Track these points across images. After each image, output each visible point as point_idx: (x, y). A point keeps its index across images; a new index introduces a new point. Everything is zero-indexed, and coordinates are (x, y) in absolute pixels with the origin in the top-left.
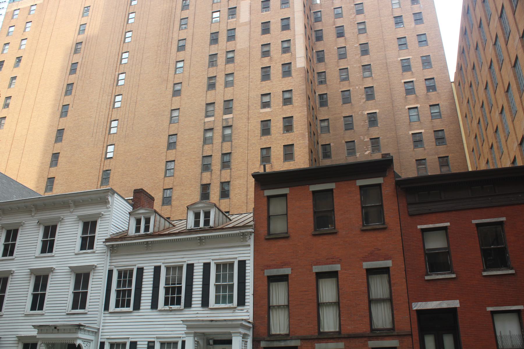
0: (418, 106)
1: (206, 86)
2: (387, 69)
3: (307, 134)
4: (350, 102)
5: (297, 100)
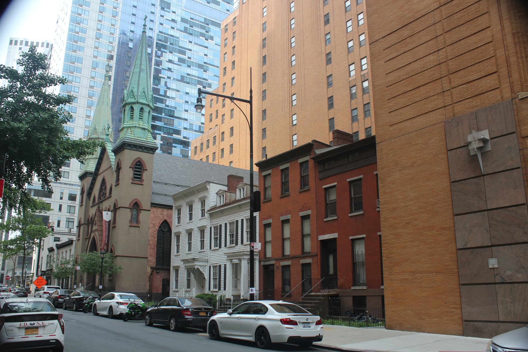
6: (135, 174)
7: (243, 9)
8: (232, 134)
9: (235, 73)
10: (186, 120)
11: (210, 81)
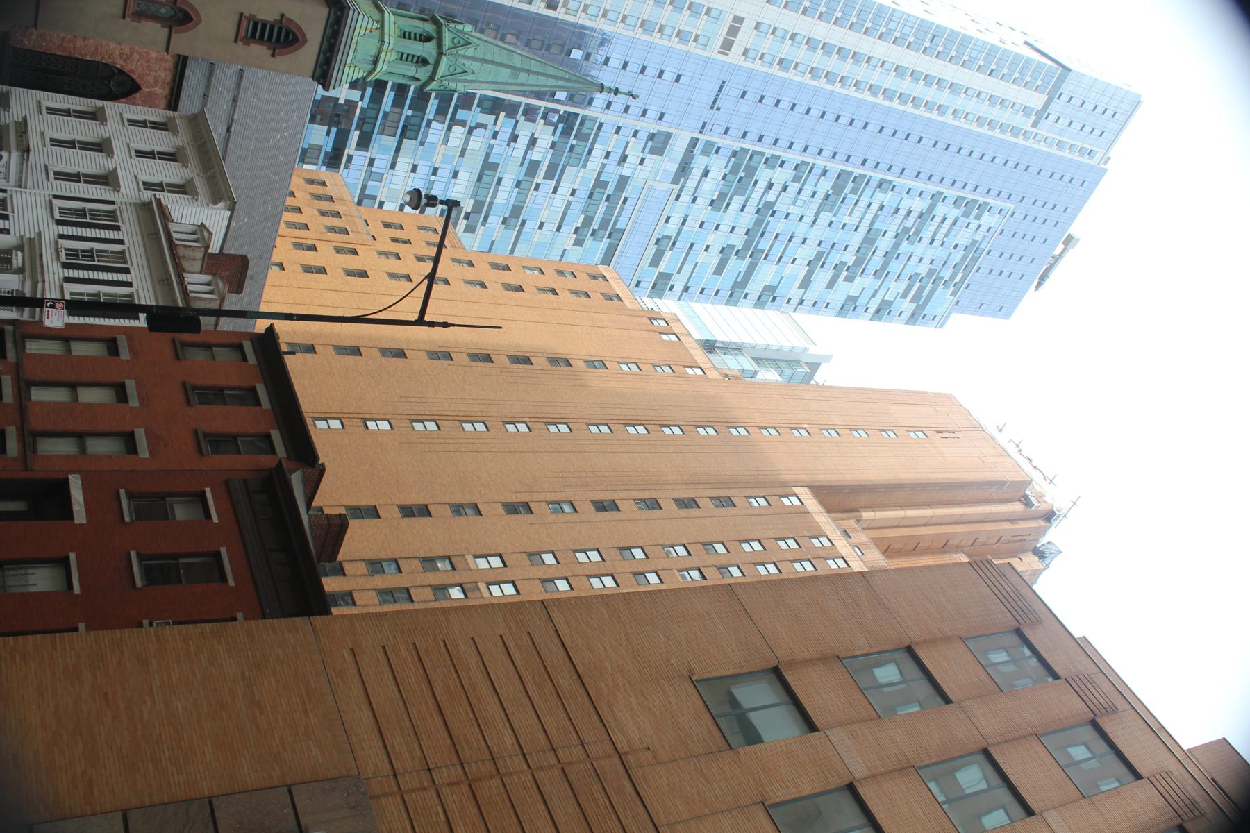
6: (264, 25)
7: (638, 319)
8: (350, 273)
9: (495, 290)
10: (393, 167)
11: (480, 230)
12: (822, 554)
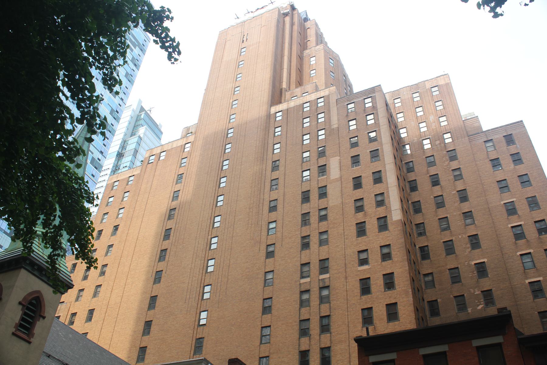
0: (531, 251)
1: (299, 246)
2: (491, 214)
3: (410, 290)
4: (454, 253)
5: (397, 254)
7: (148, 169)
12: (314, 108)
